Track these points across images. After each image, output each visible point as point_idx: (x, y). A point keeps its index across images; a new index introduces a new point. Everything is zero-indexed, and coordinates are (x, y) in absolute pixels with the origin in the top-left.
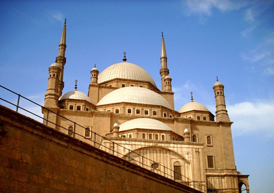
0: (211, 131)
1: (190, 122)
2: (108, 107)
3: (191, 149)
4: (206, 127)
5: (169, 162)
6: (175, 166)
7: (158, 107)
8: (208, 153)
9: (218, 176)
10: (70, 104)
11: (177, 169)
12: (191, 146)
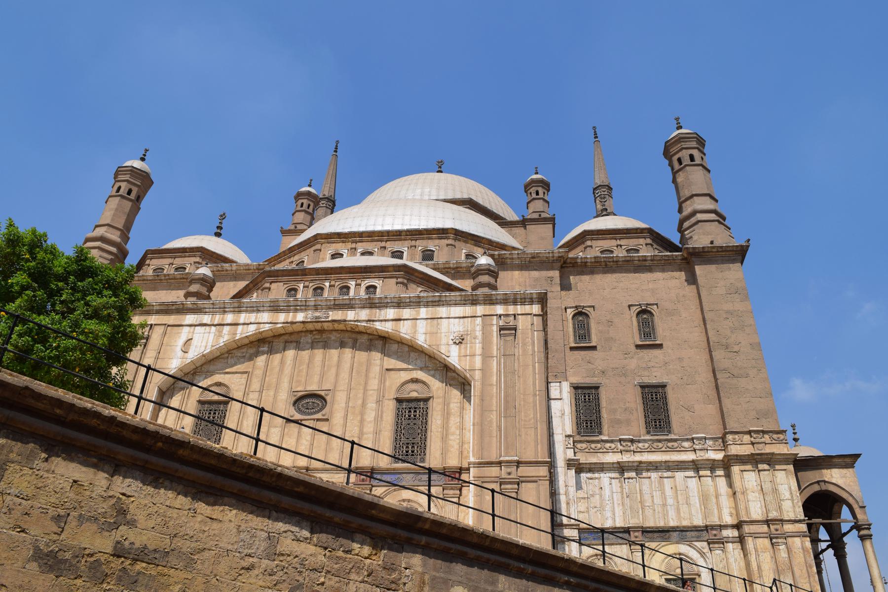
0: (653, 291)
1: (559, 264)
2: (281, 262)
3: (479, 320)
4: (631, 275)
5: (374, 384)
6: (399, 401)
7: (442, 233)
8: (646, 373)
9: (696, 466)
10: (155, 263)
11: (412, 413)
12: (480, 310)
